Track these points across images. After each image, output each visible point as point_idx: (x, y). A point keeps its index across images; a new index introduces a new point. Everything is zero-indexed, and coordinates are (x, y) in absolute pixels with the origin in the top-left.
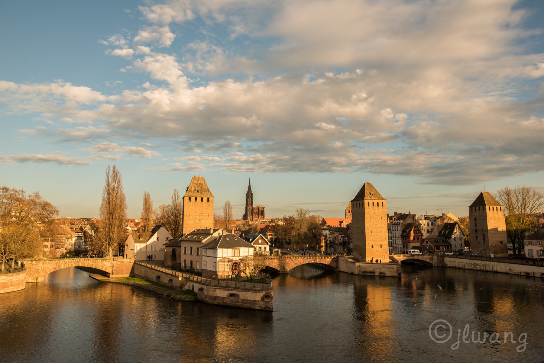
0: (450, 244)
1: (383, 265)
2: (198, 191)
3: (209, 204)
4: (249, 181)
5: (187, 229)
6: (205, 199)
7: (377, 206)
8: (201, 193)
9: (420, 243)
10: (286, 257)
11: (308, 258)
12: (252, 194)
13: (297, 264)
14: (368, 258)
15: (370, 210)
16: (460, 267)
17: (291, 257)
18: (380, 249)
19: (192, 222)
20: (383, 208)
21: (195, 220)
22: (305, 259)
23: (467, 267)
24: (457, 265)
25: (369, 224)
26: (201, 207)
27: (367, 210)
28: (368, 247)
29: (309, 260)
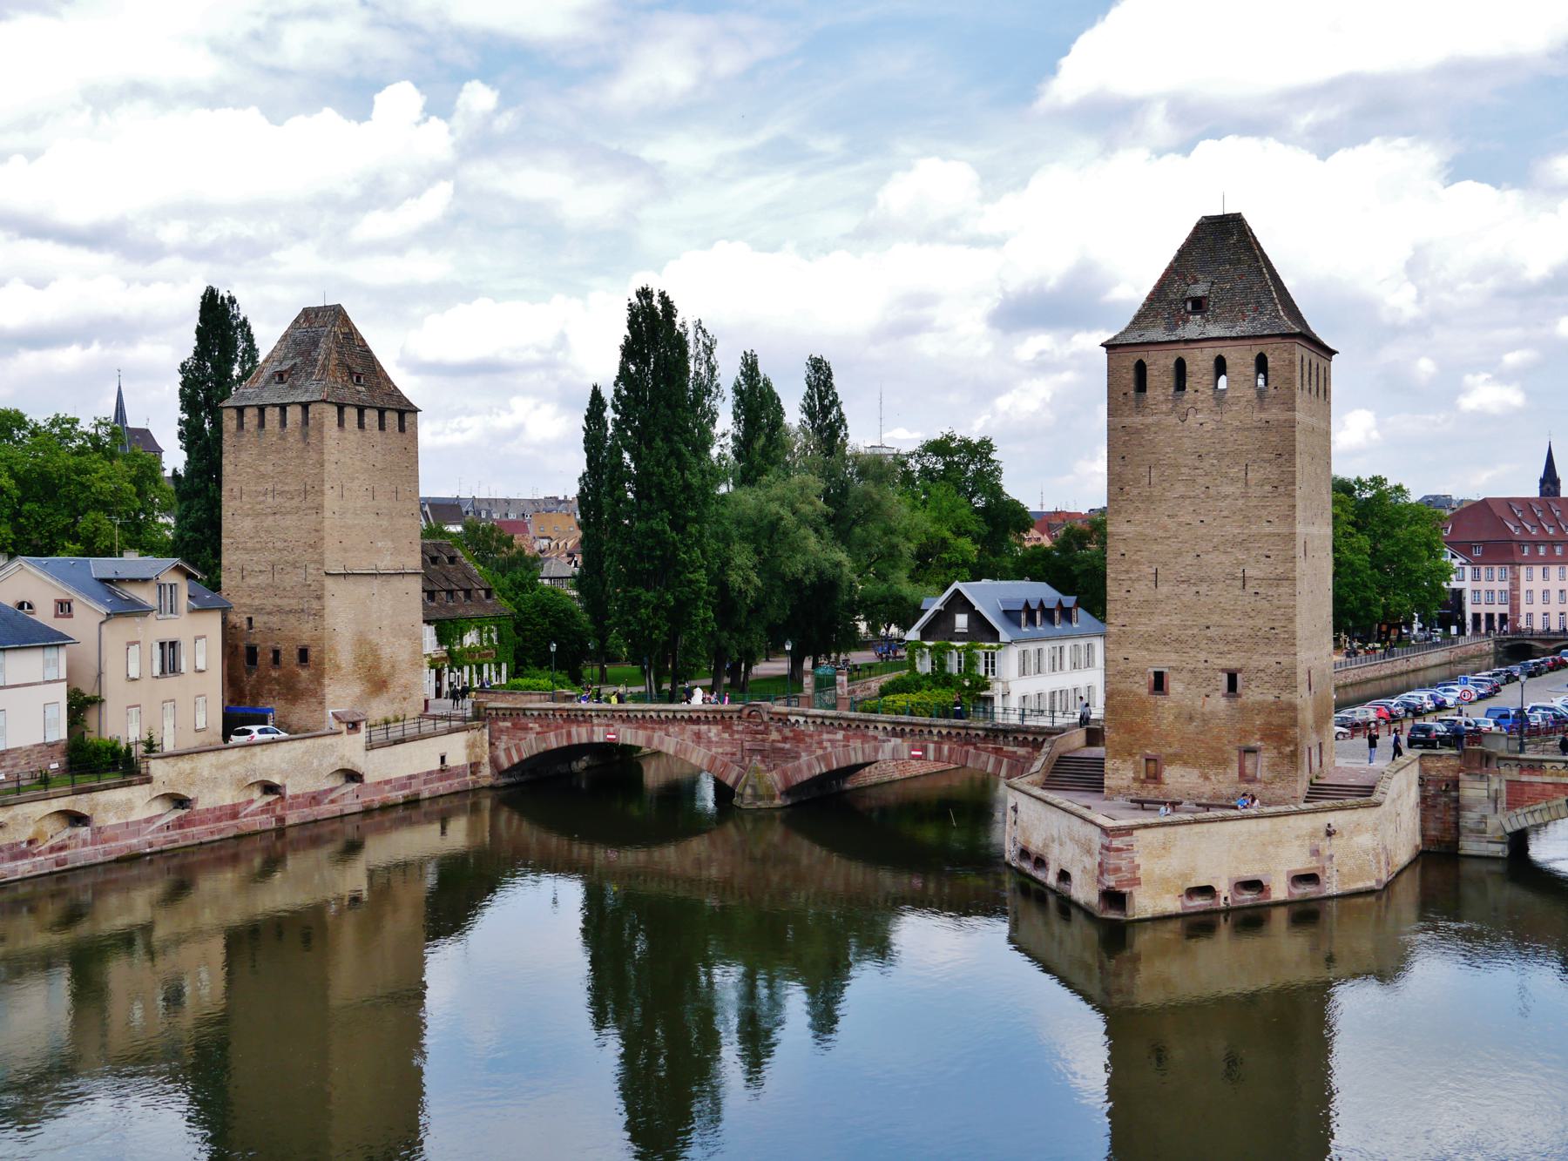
1: (1067, 815)
2: (281, 374)
3: (305, 436)
5: (235, 557)
6: (294, 414)
7: (1210, 392)
8: (293, 387)
10: (766, 718)
11: (889, 728)
13: (825, 758)
14: (1118, 763)
15: (1150, 420)
17: (793, 719)
18: (1219, 703)
19: (248, 524)
21: (258, 515)
22: (875, 738)
25: (1139, 517)
26: (279, 453)
27: (1127, 421)
28: (1122, 686)
29: (899, 741)
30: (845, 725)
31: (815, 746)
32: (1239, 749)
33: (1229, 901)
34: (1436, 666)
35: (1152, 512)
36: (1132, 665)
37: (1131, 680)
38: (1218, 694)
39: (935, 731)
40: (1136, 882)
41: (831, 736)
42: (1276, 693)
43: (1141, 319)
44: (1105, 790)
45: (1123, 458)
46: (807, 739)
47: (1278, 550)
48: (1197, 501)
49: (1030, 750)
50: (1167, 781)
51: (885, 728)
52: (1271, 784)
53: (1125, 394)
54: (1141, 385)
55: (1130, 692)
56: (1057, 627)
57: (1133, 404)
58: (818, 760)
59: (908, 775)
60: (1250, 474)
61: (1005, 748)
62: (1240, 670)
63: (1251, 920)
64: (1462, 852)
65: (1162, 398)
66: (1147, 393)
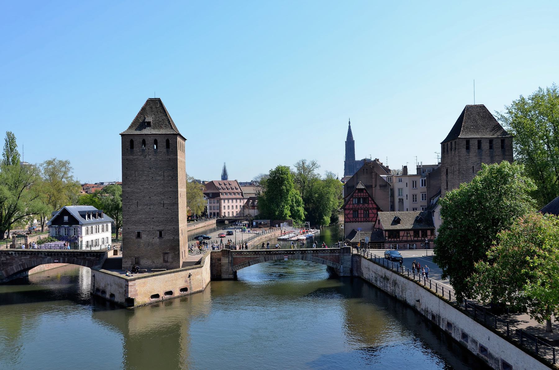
0: (432, 228)
1: (113, 276)
4: (349, 123)
9: (374, 223)
11: (46, 254)
12: (353, 142)
13: (23, 265)
15: (135, 157)
16: (373, 283)
18: (157, 240)
20: (167, 152)
22: (41, 257)
23: (379, 284)
24: (371, 277)
27: (128, 157)
28: (127, 237)
29: (50, 257)
30: (30, 253)
31: (19, 261)
32: (163, 253)
33: (163, 298)
34: (201, 227)
35: (136, 184)
36: (130, 230)
37: (130, 234)
38: (157, 238)
39: (63, 254)
40: (137, 295)
41: (25, 257)
42: (173, 236)
43: (131, 127)
44: (123, 268)
45: (127, 168)
46: (16, 259)
47: (173, 196)
48: (150, 181)
49: (94, 257)
50: (142, 264)
51: (45, 254)
52: (172, 263)
53: (127, 149)
54: (132, 146)
55: (130, 238)
56: (97, 219)
57: (130, 152)
58: (20, 266)
59: (50, 268)
60: (165, 174)
61: (87, 258)
62: (163, 230)
63: (169, 303)
64: (222, 278)
65: (138, 151)
66: (134, 149)
